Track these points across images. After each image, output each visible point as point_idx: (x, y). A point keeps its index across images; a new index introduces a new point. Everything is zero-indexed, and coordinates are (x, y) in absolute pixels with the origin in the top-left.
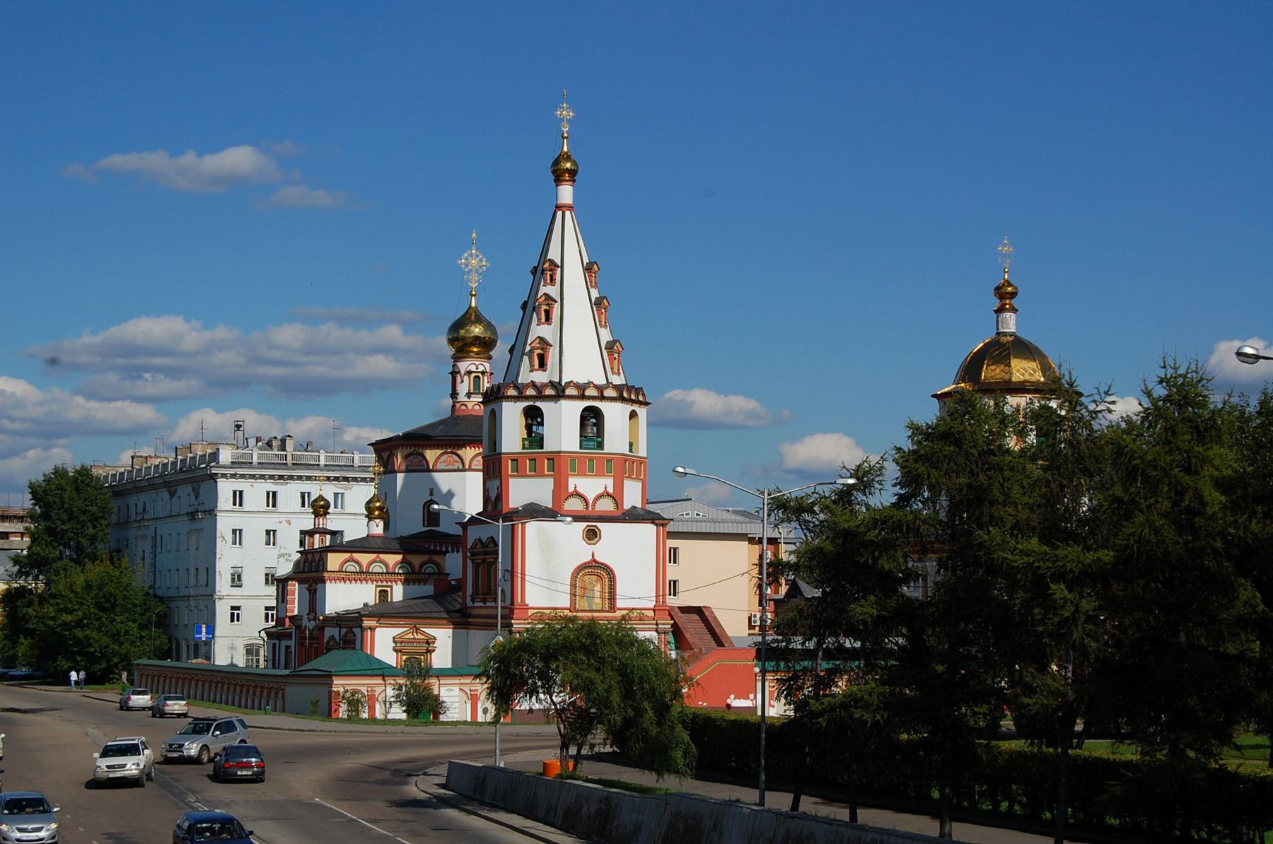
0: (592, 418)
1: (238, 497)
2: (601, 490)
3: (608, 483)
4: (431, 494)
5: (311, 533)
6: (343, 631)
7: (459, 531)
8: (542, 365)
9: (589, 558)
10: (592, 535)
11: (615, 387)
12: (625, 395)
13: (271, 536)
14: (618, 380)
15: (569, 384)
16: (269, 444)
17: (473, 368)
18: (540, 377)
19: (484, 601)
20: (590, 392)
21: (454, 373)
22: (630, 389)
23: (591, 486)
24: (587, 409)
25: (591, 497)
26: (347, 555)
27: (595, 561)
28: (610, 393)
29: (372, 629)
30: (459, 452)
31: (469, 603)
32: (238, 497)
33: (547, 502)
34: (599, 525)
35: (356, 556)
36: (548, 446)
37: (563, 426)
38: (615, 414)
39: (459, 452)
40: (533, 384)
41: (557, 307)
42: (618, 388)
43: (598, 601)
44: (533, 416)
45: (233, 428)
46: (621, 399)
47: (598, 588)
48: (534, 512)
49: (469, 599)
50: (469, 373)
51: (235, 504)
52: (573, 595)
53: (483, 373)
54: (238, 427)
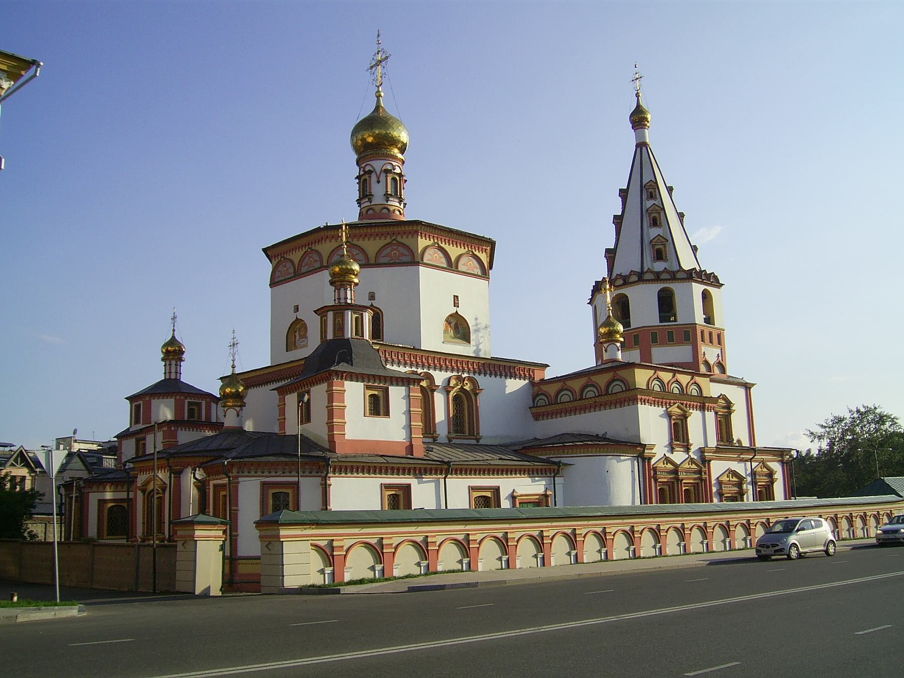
8: (659, 255)
25: (711, 363)
41: (662, 213)
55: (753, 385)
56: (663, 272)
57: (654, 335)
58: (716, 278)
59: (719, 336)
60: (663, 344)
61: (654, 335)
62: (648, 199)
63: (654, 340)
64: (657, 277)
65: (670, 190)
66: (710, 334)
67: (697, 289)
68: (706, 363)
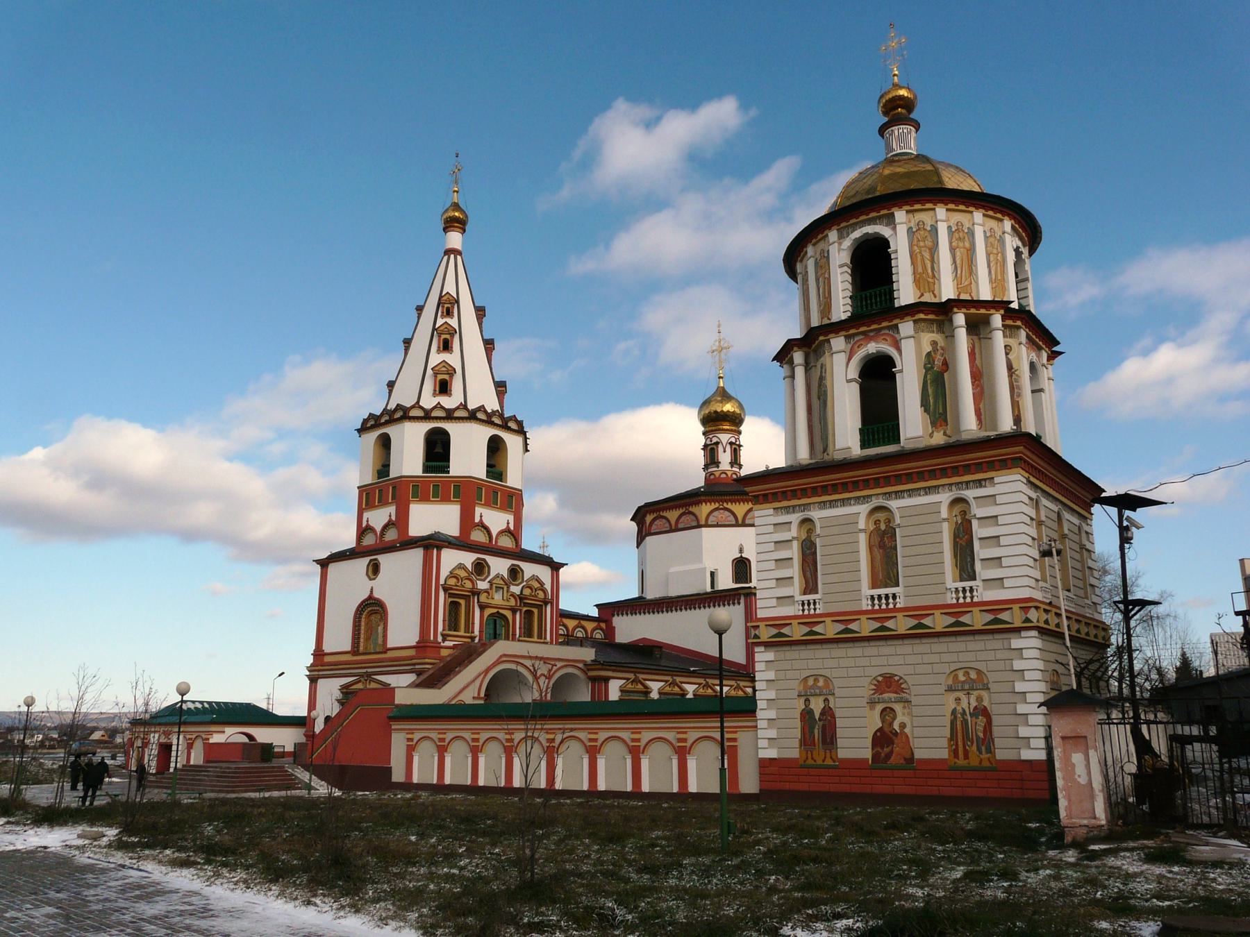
0: (495, 448)
2: (504, 527)
23: (496, 520)
41: (457, 337)
55: (564, 565)
56: (435, 407)
58: (520, 423)
60: (425, 499)
62: (442, 316)
65: (480, 312)
67: (482, 434)
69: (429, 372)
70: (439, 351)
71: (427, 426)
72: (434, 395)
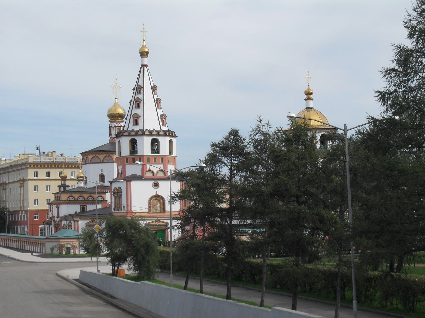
0: (155, 143)
1: (36, 174)
3: (161, 166)
4: (102, 171)
5: (60, 187)
6: (68, 222)
7: (109, 185)
8: (136, 123)
9: (155, 194)
10: (156, 185)
11: (164, 131)
12: (167, 134)
13: (48, 188)
14: (164, 128)
15: (147, 130)
16: (47, 155)
17: (117, 125)
18: (136, 128)
19: (118, 210)
20: (154, 133)
21: (110, 127)
22: (169, 131)
23: (155, 168)
24: (153, 139)
26: (69, 195)
27: (157, 195)
28: (161, 133)
29: (77, 221)
30: (112, 155)
31: (113, 211)
32: (36, 174)
33: (139, 173)
34: (159, 182)
35: (73, 195)
36: (139, 153)
37: (145, 146)
38: (164, 142)
39: (112, 155)
40: (133, 131)
42: (165, 132)
43: (159, 208)
44: (133, 144)
45: (36, 149)
46: (165, 135)
47: (158, 205)
48: (135, 178)
49: (113, 209)
50: (116, 127)
51: (35, 176)
52: (149, 208)
53: (120, 127)
54: (37, 148)
57: (127, 159)
59: (162, 158)
60: (130, 164)
61: (127, 159)
63: (127, 162)
64: (129, 135)
66: (155, 158)
68: (150, 171)
69: (132, 117)
70: (136, 108)
71: (129, 138)
72: (133, 125)
